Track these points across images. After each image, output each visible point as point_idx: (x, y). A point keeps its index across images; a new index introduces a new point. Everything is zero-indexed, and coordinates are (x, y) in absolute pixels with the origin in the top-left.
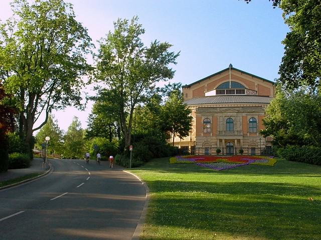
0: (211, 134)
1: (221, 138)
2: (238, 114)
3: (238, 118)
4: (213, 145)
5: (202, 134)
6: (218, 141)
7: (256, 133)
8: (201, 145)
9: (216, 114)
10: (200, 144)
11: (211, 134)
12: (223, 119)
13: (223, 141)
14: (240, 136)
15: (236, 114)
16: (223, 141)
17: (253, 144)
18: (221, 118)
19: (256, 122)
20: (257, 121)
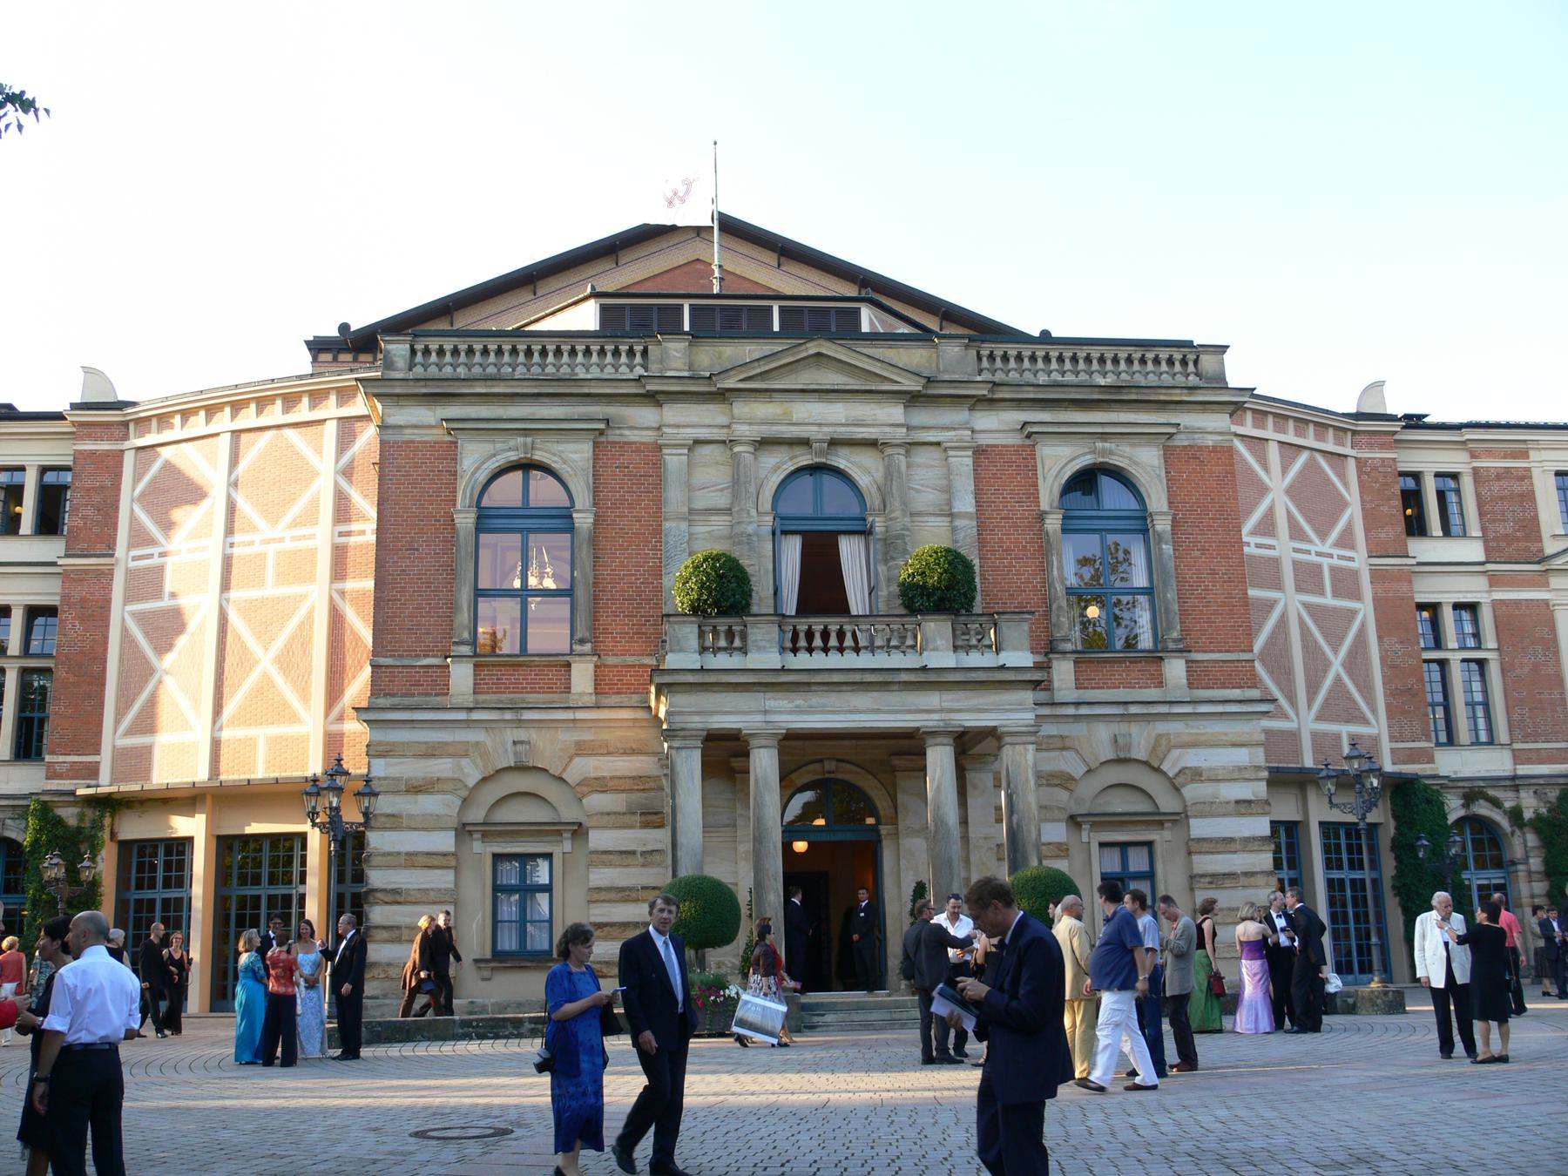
0: (582, 677)
1: (732, 713)
2: (922, 416)
3: (924, 473)
4: (616, 820)
5: (461, 676)
6: (690, 764)
7: (1156, 657)
8: (430, 824)
9: (645, 415)
10: (428, 804)
11: (582, 677)
12: (736, 484)
13: (764, 764)
14: (998, 681)
15: (895, 412)
16: (764, 764)
17: (1120, 804)
18: (712, 472)
19: (1141, 523)
20: (1157, 501)
